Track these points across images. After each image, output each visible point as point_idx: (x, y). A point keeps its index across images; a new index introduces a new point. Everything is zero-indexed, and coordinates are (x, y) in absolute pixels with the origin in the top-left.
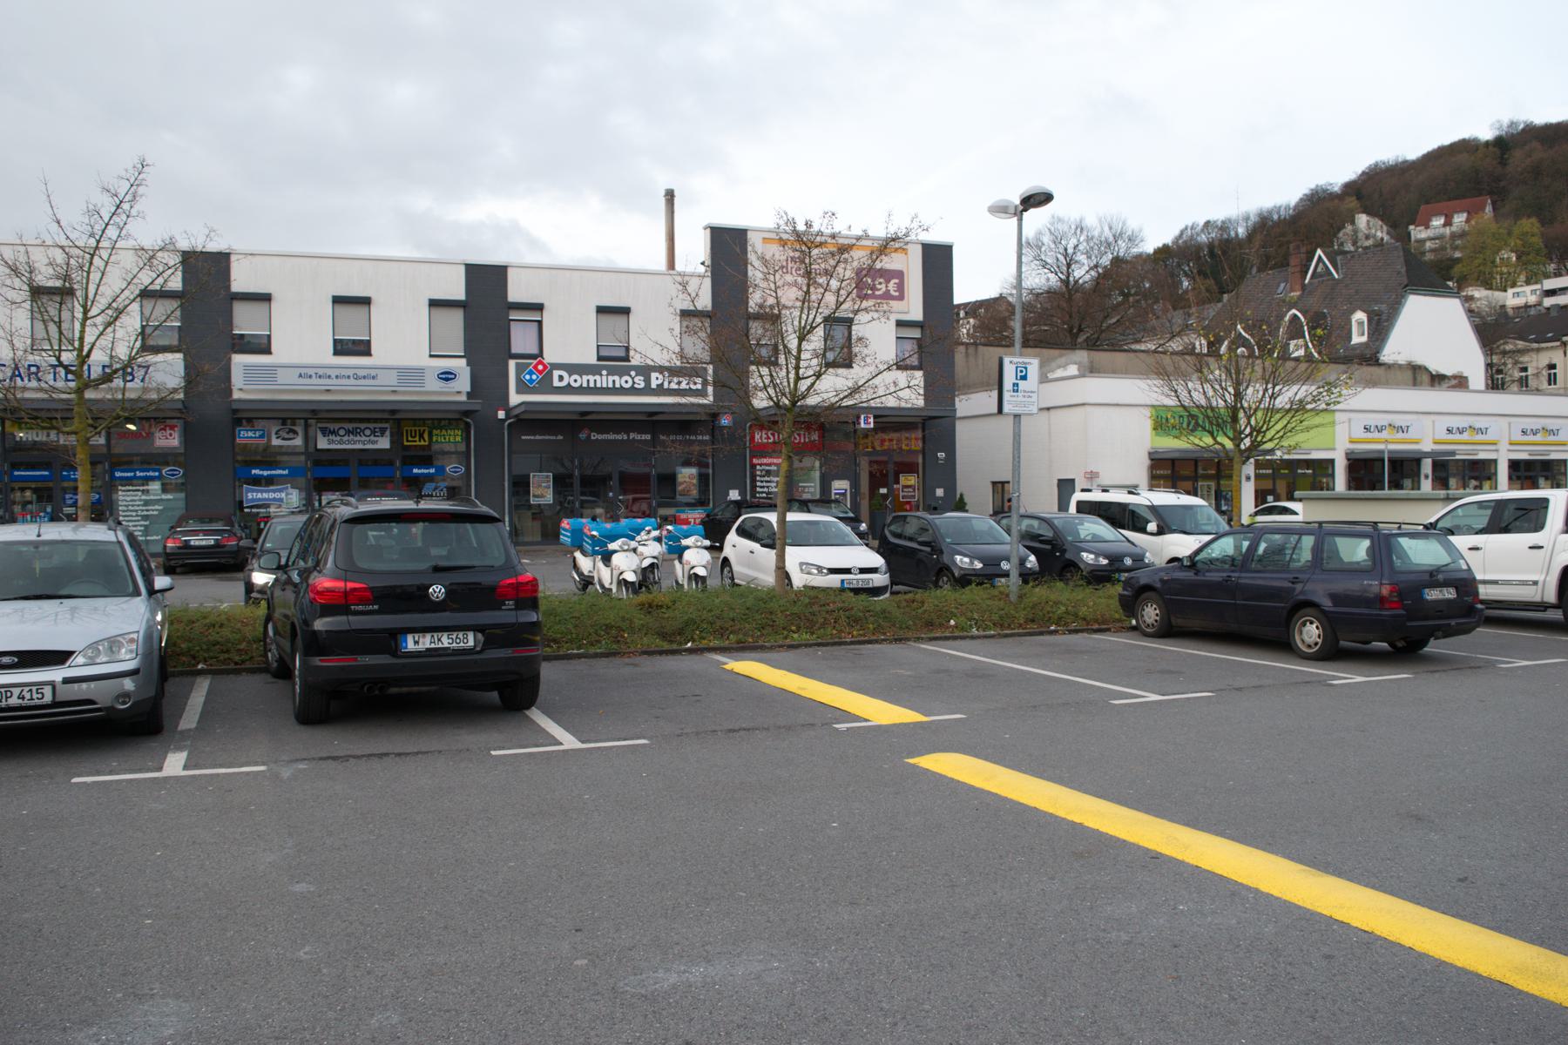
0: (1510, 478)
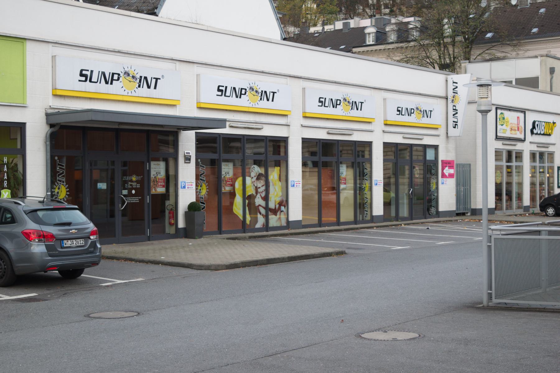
0: (304, 164)
